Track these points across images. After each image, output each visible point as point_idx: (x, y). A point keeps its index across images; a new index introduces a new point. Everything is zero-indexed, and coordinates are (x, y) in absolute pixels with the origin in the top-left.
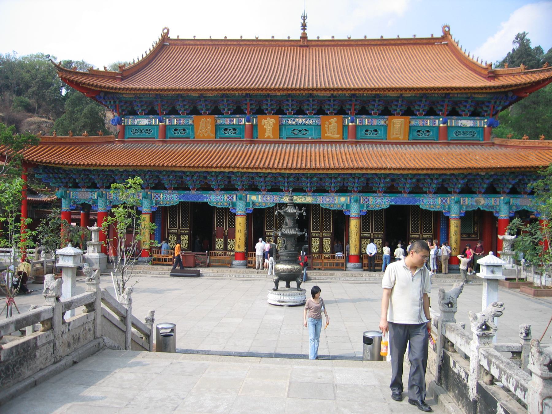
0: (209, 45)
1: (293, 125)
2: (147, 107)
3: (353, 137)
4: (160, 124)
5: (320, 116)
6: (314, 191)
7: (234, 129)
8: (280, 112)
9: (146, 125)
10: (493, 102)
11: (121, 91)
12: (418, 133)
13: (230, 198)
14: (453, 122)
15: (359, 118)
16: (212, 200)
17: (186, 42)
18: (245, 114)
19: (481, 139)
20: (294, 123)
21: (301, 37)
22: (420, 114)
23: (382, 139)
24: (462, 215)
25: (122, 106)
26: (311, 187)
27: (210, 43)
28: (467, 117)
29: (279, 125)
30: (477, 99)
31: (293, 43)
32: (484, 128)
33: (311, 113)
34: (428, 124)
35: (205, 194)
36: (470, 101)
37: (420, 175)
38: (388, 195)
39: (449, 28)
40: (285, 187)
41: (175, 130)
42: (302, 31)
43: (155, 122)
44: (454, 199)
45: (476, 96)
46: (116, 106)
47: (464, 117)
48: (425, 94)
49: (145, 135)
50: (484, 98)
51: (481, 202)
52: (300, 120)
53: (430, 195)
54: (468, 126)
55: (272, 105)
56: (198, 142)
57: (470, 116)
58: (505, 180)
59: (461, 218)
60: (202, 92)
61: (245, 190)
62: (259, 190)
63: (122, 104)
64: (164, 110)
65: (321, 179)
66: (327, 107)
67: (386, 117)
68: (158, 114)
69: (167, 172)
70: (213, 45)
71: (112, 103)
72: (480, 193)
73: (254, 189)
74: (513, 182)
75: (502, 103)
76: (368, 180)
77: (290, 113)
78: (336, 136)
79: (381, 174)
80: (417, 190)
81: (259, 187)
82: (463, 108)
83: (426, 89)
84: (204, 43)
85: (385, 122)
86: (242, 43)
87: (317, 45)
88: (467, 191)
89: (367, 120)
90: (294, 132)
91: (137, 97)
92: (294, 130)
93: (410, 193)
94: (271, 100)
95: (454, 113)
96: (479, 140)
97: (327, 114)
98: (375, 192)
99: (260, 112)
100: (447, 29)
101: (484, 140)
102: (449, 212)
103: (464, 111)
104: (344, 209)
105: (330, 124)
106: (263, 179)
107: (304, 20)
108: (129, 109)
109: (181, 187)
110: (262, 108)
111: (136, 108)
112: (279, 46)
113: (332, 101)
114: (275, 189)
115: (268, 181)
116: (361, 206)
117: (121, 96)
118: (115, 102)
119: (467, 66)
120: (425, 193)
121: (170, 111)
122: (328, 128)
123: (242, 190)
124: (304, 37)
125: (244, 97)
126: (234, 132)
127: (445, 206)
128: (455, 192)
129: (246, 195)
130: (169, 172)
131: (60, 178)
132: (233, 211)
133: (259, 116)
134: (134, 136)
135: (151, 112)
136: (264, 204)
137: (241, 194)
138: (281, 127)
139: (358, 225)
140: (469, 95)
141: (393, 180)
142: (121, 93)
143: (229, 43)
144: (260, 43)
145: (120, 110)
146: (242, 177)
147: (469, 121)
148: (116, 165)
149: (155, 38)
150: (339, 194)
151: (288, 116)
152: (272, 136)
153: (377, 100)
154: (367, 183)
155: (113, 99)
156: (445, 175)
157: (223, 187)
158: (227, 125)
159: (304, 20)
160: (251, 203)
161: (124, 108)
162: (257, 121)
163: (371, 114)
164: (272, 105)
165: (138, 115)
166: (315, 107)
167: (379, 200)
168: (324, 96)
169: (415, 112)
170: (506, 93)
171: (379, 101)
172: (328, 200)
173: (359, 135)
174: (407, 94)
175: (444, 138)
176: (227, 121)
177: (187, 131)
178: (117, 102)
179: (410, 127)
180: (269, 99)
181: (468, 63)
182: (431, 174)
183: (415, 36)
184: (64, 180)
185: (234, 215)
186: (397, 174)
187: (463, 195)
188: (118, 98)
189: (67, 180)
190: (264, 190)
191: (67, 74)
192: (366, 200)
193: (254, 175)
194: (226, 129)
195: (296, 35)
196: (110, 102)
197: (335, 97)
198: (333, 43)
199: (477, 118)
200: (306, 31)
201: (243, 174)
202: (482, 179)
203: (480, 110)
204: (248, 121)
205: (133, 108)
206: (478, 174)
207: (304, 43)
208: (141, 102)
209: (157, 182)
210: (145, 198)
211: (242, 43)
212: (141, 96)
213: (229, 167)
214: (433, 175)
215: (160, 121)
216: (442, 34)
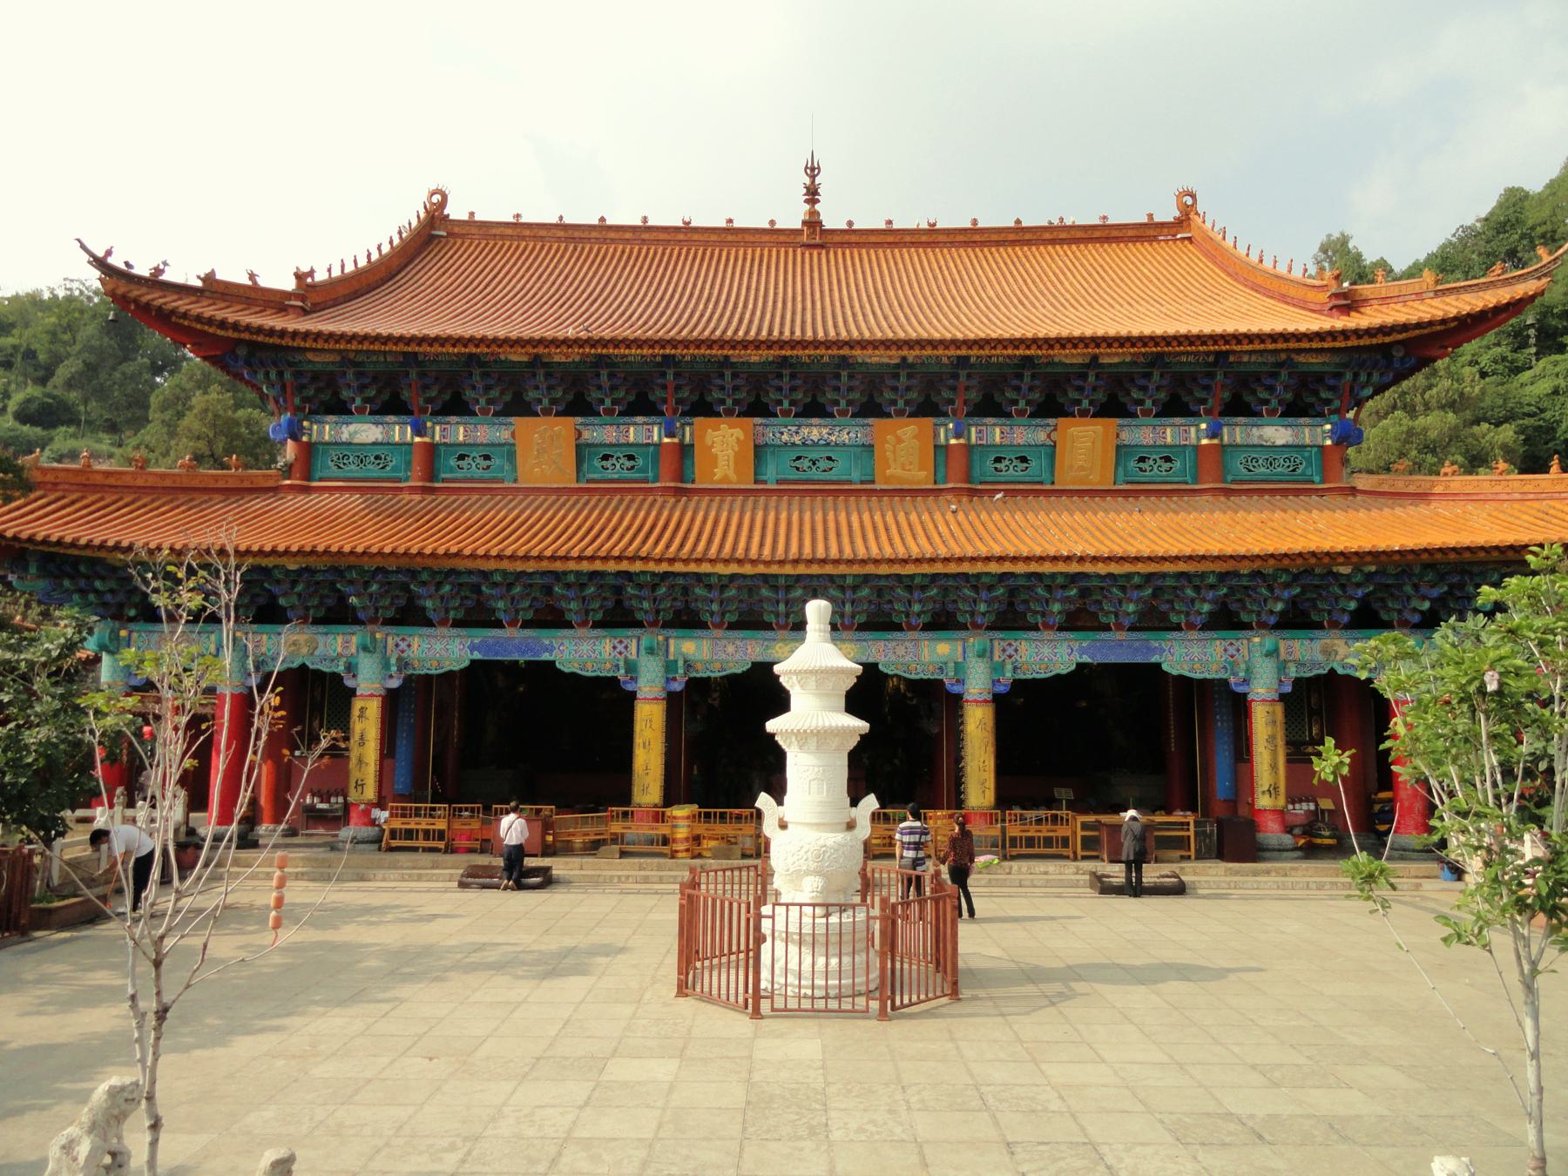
0: (559, 240)
1: (793, 444)
2: (379, 392)
3: (966, 479)
4: (417, 439)
5: (870, 421)
6: (863, 627)
7: (631, 458)
8: (757, 408)
9: (374, 444)
10: (1349, 376)
11: (298, 343)
12: (1141, 465)
13: (620, 648)
14: (1237, 432)
15: (977, 425)
16: (566, 656)
17: (494, 231)
18: (661, 414)
19: (1317, 479)
20: (797, 440)
21: (804, 223)
22: (1146, 413)
23: (1041, 483)
24: (1288, 689)
25: (303, 387)
26: (853, 616)
27: (561, 234)
28: (1276, 419)
29: (756, 446)
30: (1305, 369)
31: (782, 238)
32: (1322, 447)
33: (843, 413)
34: (1169, 440)
35: (546, 637)
36: (1284, 374)
37: (1164, 575)
38: (1071, 635)
39: (1193, 196)
40: (777, 615)
41: (462, 457)
42: (807, 207)
43: (403, 433)
44: (1261, 644)
45: (1301, 359)
46: (284, 387)
47: (1266, 419)
48: (1161, 355)
49: (373, 470)
50: (1323, 364)
52: (815, 431)
53: (1194, 635)
54: (1279, 442)
55: (736, 388)
57: (1283, 415)
58: (1408, 589)
59: (1283, 698)
60: (541, 350)
61: (664, 627)
62: (703, 626)
63: (305, 381)
64: (429, 401)
65: (880, 592)
66: (888, 395)
67: (1052, 421)
68: (409, 413)
69: (434, 573)
70: (569, 240)
71: (273, 376)
72: (1334, 625)
73: (688, 620)
74: (1435, 593)
75: (1376, 377)
76: (1012, 592)
77: (786, 414)
78: (920, 476)
79: (1053, 576)
80: (1154, 620)
81: (706, 617)
82: (1263, 395)
83: (1167, 340)
84: (542, 233)
85: (1049, 436)
86: (646, 236)
87: (850, 245)
88: (1296, 620)
89: (998, 430)
90: (797, 464)
91: (346, 361)
92: (799, 458)
93: (1132, 629)
94: (735, 376)
95: (1238, 408)
96: (1313, 482)
97: (889, 415)
98: (1036, 628)
99: (703, 408)
100: (1189, 201)
101: (1323, 481)
102: (1246, 681)
103: (1267, 402)
104: (948, 678)
105: (899, 440)
106: (714, 594)
107: (813, 177)
108: (326, 396)
109: (477, 617)
110: (709, 399)
111: (345, 394)
112: (746, 244)
113: (903, 379)
115: (730, 600)
116: (997, 668)
117: (299, 357)
118: (280, 374)
119: (1256, 288)
120: (1178, 628)
121: (445, 404)
122: (894, 452)
123: (654, 624)
124: (813, 223)
125: (659, 365)
126: (629, 464)
127: (1236, 663)
128: (1262, 625)
129: (667, 639)
130: (440, 572)
131: (96, 591)
132: (629, 688)
133: (698, 420)
134: (340, 474)
135: (390, 406)
136: (718, 665)
137: (649, 637)
138: (760, 451)
139: (990, 723)
140: (1283, 356)
141: (1084, 593)
142: (299, 349)
143: (612, 235)
144: (696, 237)
145: (297, 401)
146: (655, 587)
147: (1282, 429)
148: (274, 552)
149: (407, 213)
150: (930, 634)
151: (781, 420)
152: (733, 477)
153: (1027, 374)
154: (1011, 604)
155: (275, 364)
156: (1236, 574)
157: (599, 616)
158: (611, 445)
159: (813, 177)
160: (680, 663)
161: (312, 392)
163: (1008, 415)
164: (736, 388)
165: (350, 413)
166: (856, 395)
167: (1046, 650)
168: (882, 365)
169: (1132, 408)
170: (1385, 349)
171: (1033, 376)
172: (901, 651)
173: (976, 472)
174: (1110, 358)
175: (1219, 478)
177: (496, 462)
178: (287, 376)
179: (1118, 447)
180: (728, 374)
181: (1259, 281)
182: (1196, 575)
183: (1105, 218)
184: (108, 597)
185: (632, 696)
186: (1098, 576)
187: (1287, 633)
188: (291, 364)
189: (121, 597)
190: (718, 626)
191: (132, 286)
192: (1010, 651)
193: (690, 581)
194: (606, 457)
195: (792, 216)
196: (267, 374)
197: (912, 366)
198: (890, 239)
199: (1302, 420)
200: (817, 207)
201: (657, 580)
202: (1343, 587)
203: (1311, 399)
204: (670, 435)
205: (336, 394)
206: (1330, 573)
207: (815, 237)
208: (359, 375)
209: (402, 602)
210: (365, 649)
211: (646, 236)
212: (360, 359)
213: (619, 558)
214: (1203, 575)
215: (419, 430)
216: (1177, 214)
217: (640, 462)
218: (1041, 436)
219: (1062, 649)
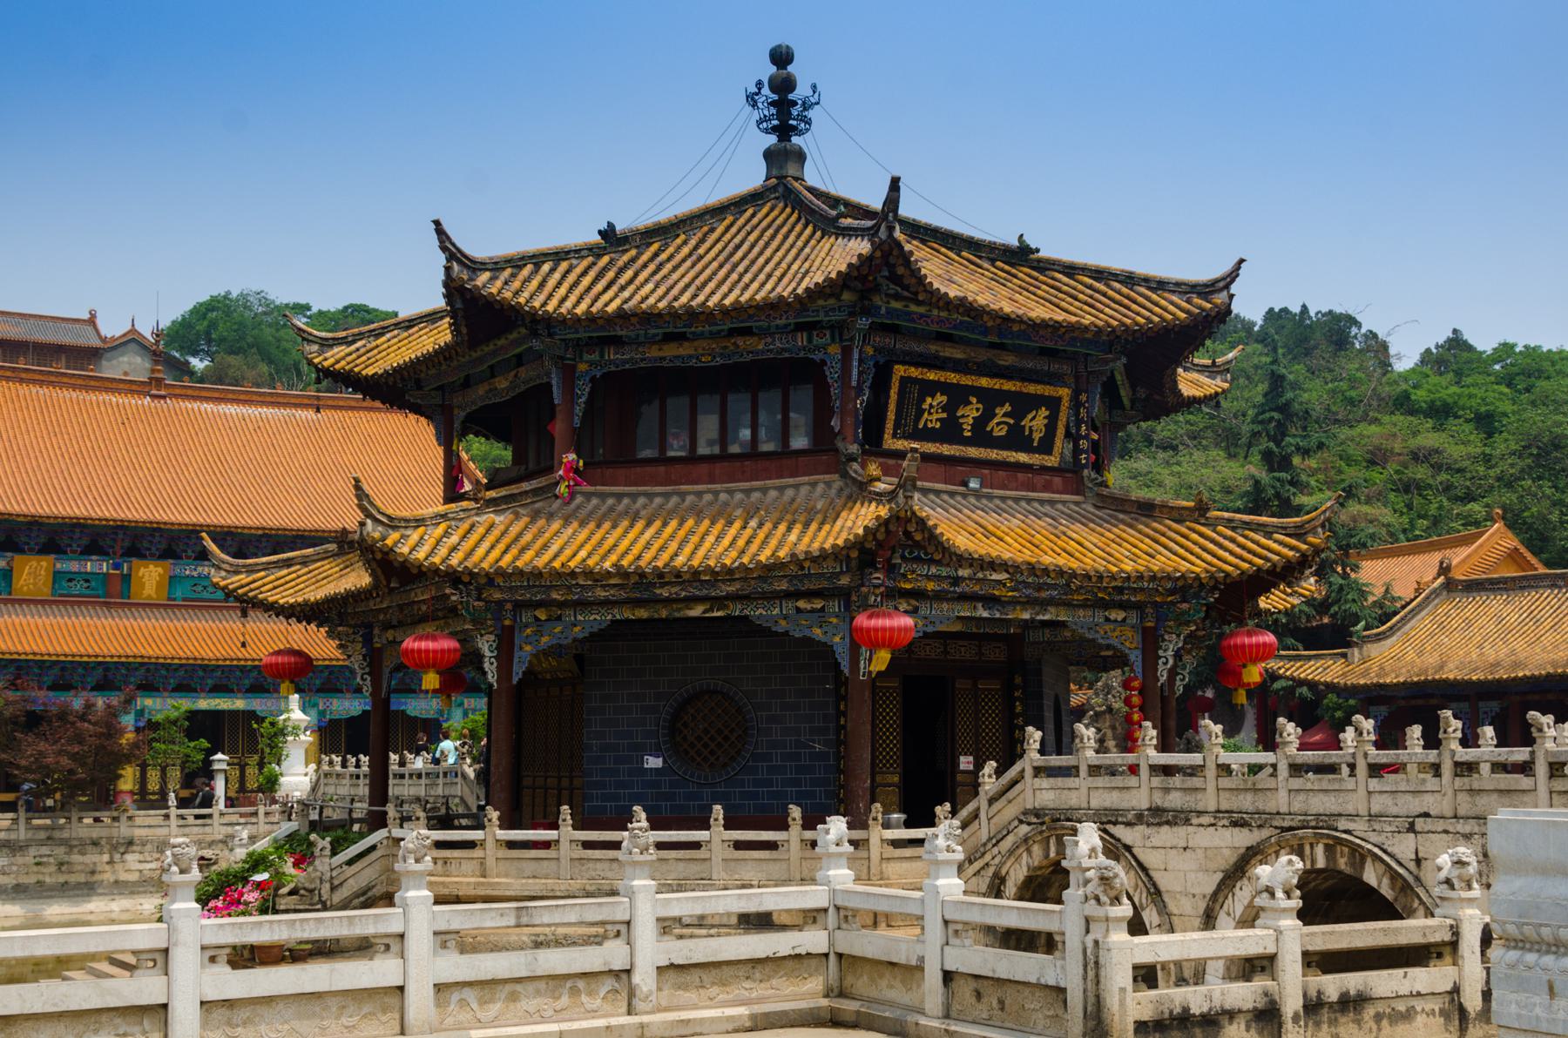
6: (248, 691)
7: (87, 581)
56: (21, 602)
114: (183, 688)
133: (134, 560)
138: (173, 579)
162: (130, 569)
167: (347, 703)
176: (73, 566)
194: (70, 580)
217: (93, 584)
219: (356, 703)
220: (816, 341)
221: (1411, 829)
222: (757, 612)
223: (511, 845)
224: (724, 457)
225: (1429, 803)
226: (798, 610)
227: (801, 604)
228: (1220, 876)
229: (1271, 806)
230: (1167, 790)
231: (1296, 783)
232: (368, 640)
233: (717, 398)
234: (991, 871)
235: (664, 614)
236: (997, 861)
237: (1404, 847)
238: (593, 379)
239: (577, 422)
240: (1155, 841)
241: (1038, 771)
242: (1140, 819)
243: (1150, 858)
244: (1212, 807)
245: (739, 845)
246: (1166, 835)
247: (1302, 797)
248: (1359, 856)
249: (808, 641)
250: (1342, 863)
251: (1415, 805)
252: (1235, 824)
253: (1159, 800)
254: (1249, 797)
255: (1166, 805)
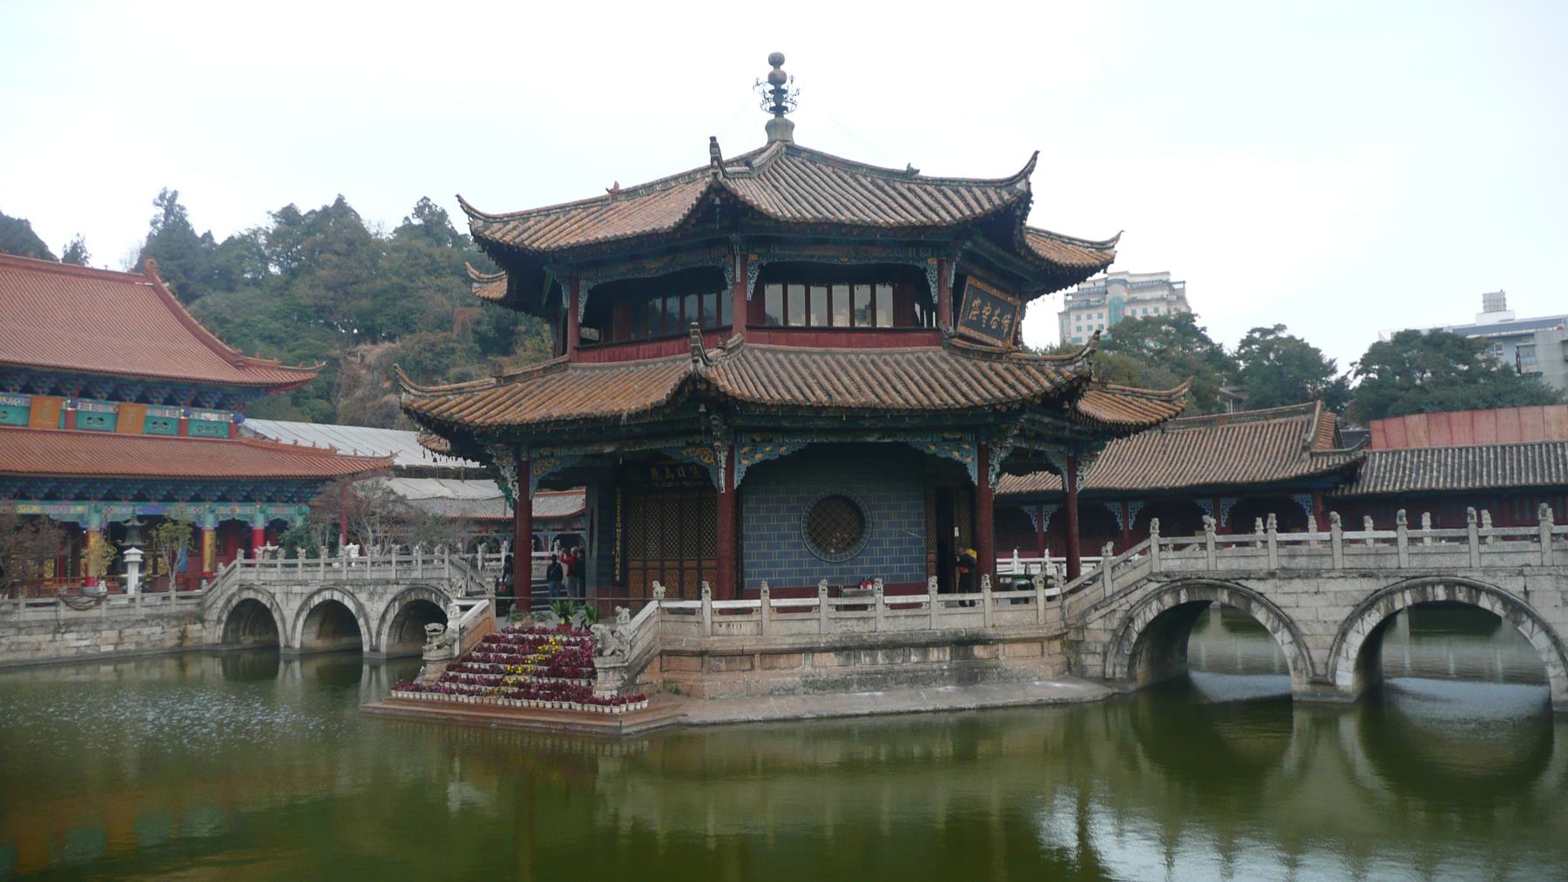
51: (238, 511)
95: (196, 404)
218: (111, 409)
220: (922, 254)
221: (1521, 573)
222: (915, 441)
223: (782, 610)
224: (852, 330)
225: (1533, 559)
226: (945, 440)
227: (946, 435)
228: (1348, 611)
229: (1392, 563)
230: (1293, 556)
231: (1412, 549)
232: (517, 456)
233: (847, 288)
234: (1119, 614)
235: (849, 439)
236: (1127, 607)
237: (1514, 587)
238: (761, 267)
239: (749, 296)
240: (1286, 589)
241: (1162, 547)
242: (1272, 575)
243: (1279, 600)
244: (1339, 565)
245: (948, 604)
246: (1297, 585)
247: (1418, 558)
248: (1476, 589)
249: (950, 460)
250: (1461, 596)
251: (1519, 560)
252: (1364, 576)
253: (1284, 562)
254: (1372, 559)
255: (1293, 566)
